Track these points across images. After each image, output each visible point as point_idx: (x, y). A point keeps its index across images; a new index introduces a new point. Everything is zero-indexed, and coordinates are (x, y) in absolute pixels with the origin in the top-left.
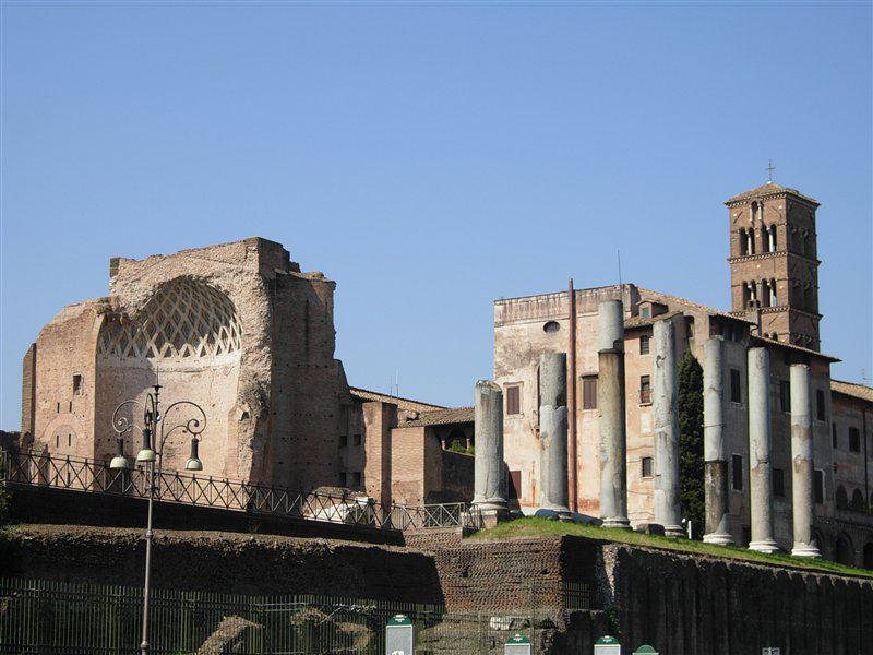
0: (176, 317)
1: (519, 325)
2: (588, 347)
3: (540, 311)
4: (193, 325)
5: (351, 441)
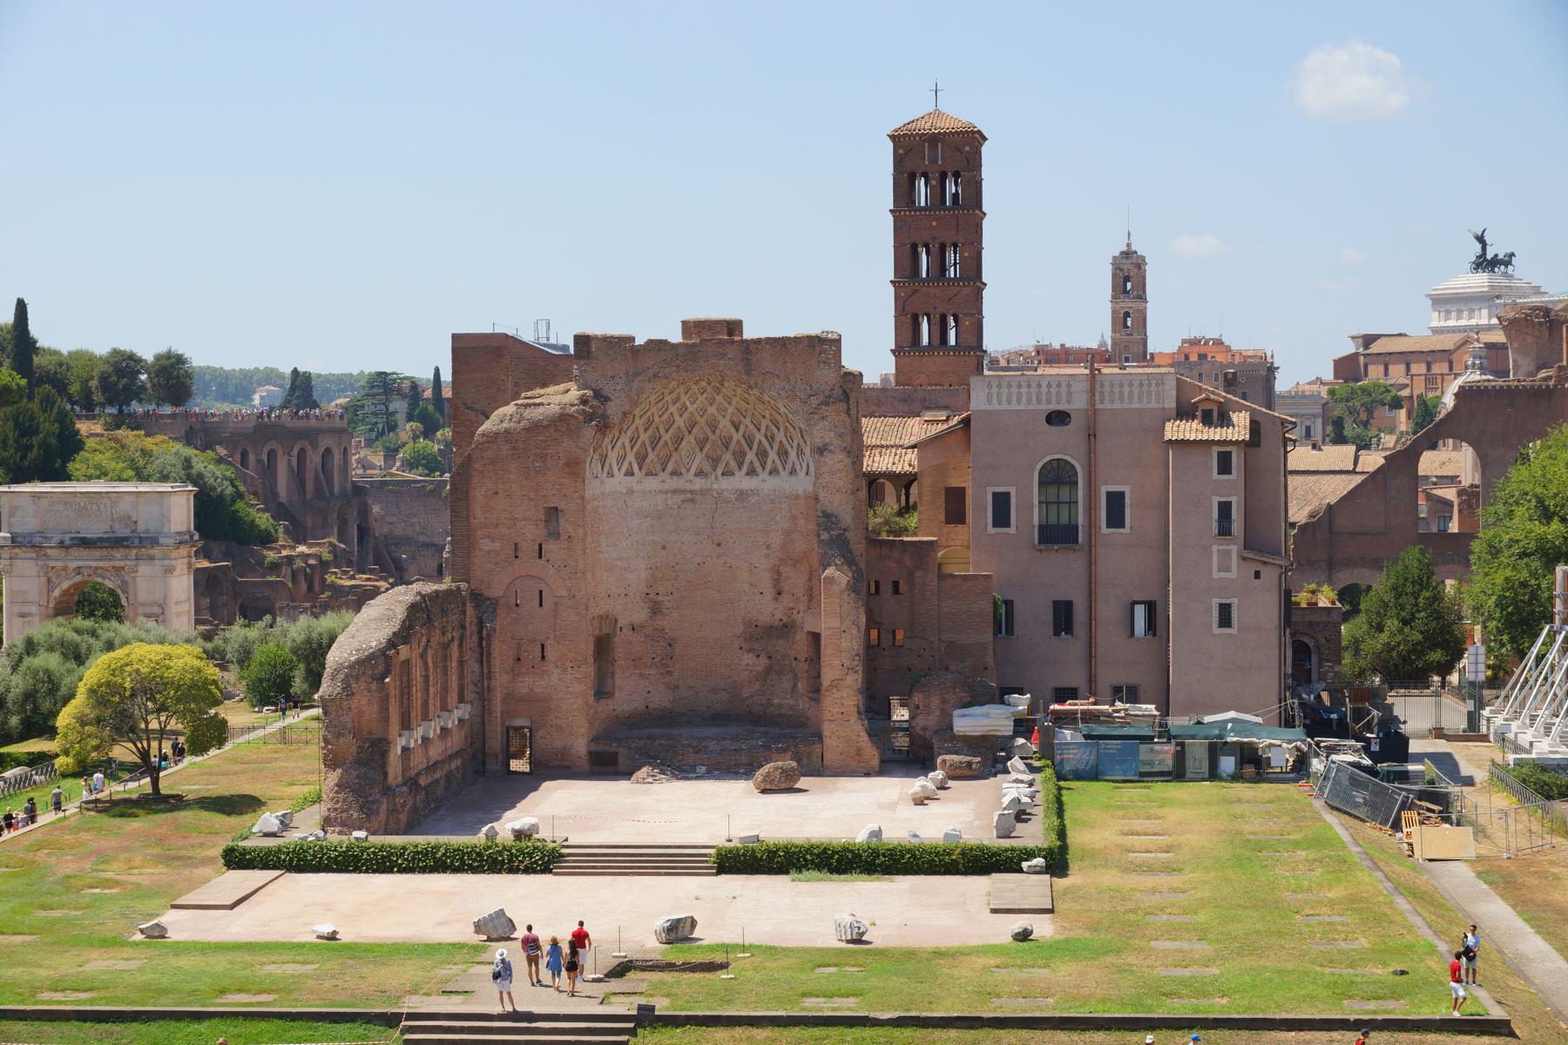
0: (670, 424)
4: (690, 432)
5: (886, 588)
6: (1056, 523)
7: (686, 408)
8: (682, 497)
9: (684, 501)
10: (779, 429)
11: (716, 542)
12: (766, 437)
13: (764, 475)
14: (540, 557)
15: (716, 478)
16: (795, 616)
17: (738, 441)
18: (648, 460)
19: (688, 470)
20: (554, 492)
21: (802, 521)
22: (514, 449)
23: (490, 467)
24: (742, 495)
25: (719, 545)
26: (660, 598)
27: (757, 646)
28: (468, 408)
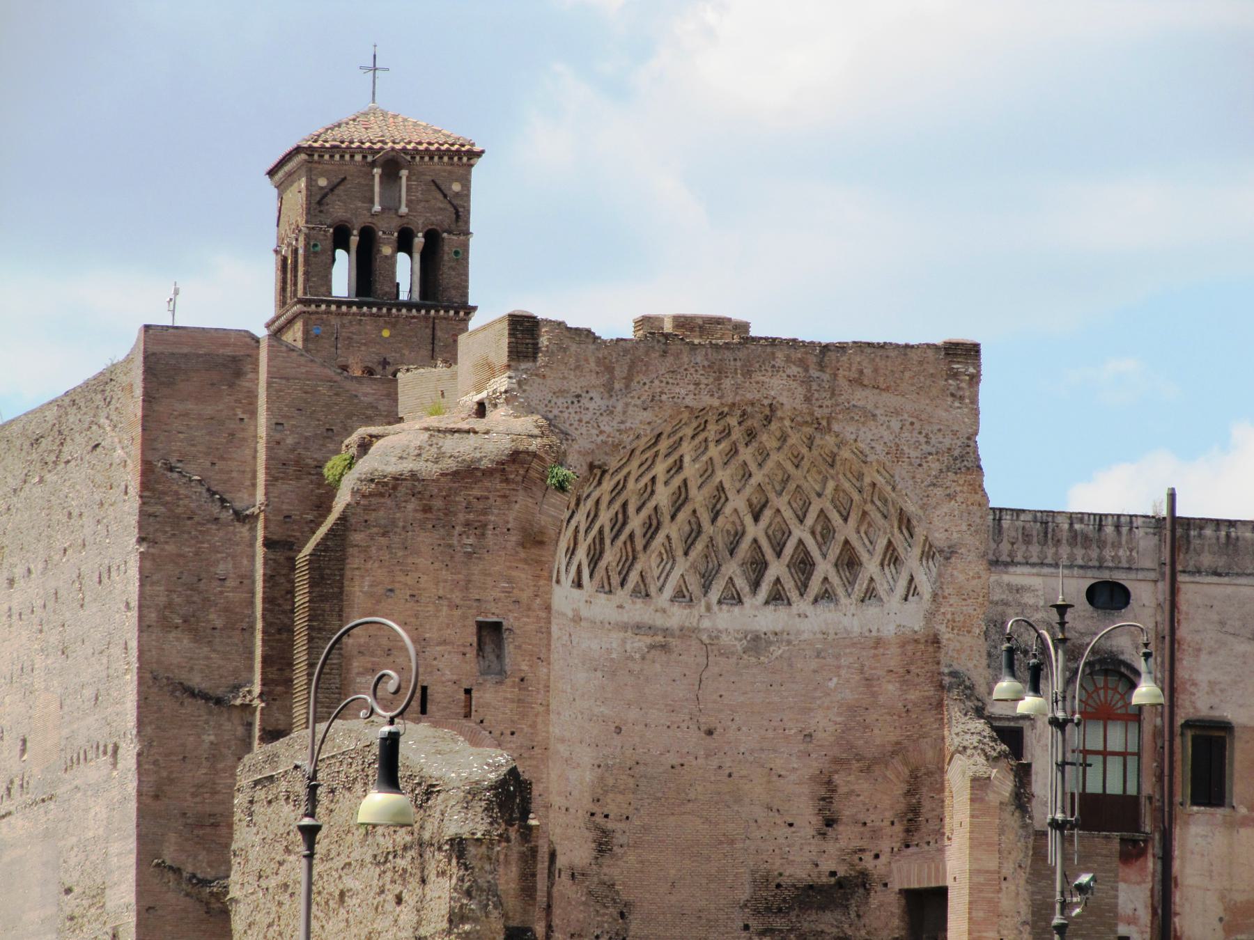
1: (1019, 576)
2: (1204, 656)
3: (1079, 552)
4: (673, 517)
6: (1100, 791)
7: (681, 468)
8: (649, 640)
9: (652, 647)
10: (846, 520)
11: (704, 728)
12: (813, 533)
13: (801, 605)
14: (467, 715)
15: (709, 608)
16: (869, 863)
17: (755, 541)
18: (602, 564)
19: (661, 589)
20: (496, 593)
21: (890, 689)
22: (427, 509)
23: (383, 541)
24: (757, 642)
25: (710, 733)
26: (610, 825)
27: (779, 923)
28: (171, 469)
